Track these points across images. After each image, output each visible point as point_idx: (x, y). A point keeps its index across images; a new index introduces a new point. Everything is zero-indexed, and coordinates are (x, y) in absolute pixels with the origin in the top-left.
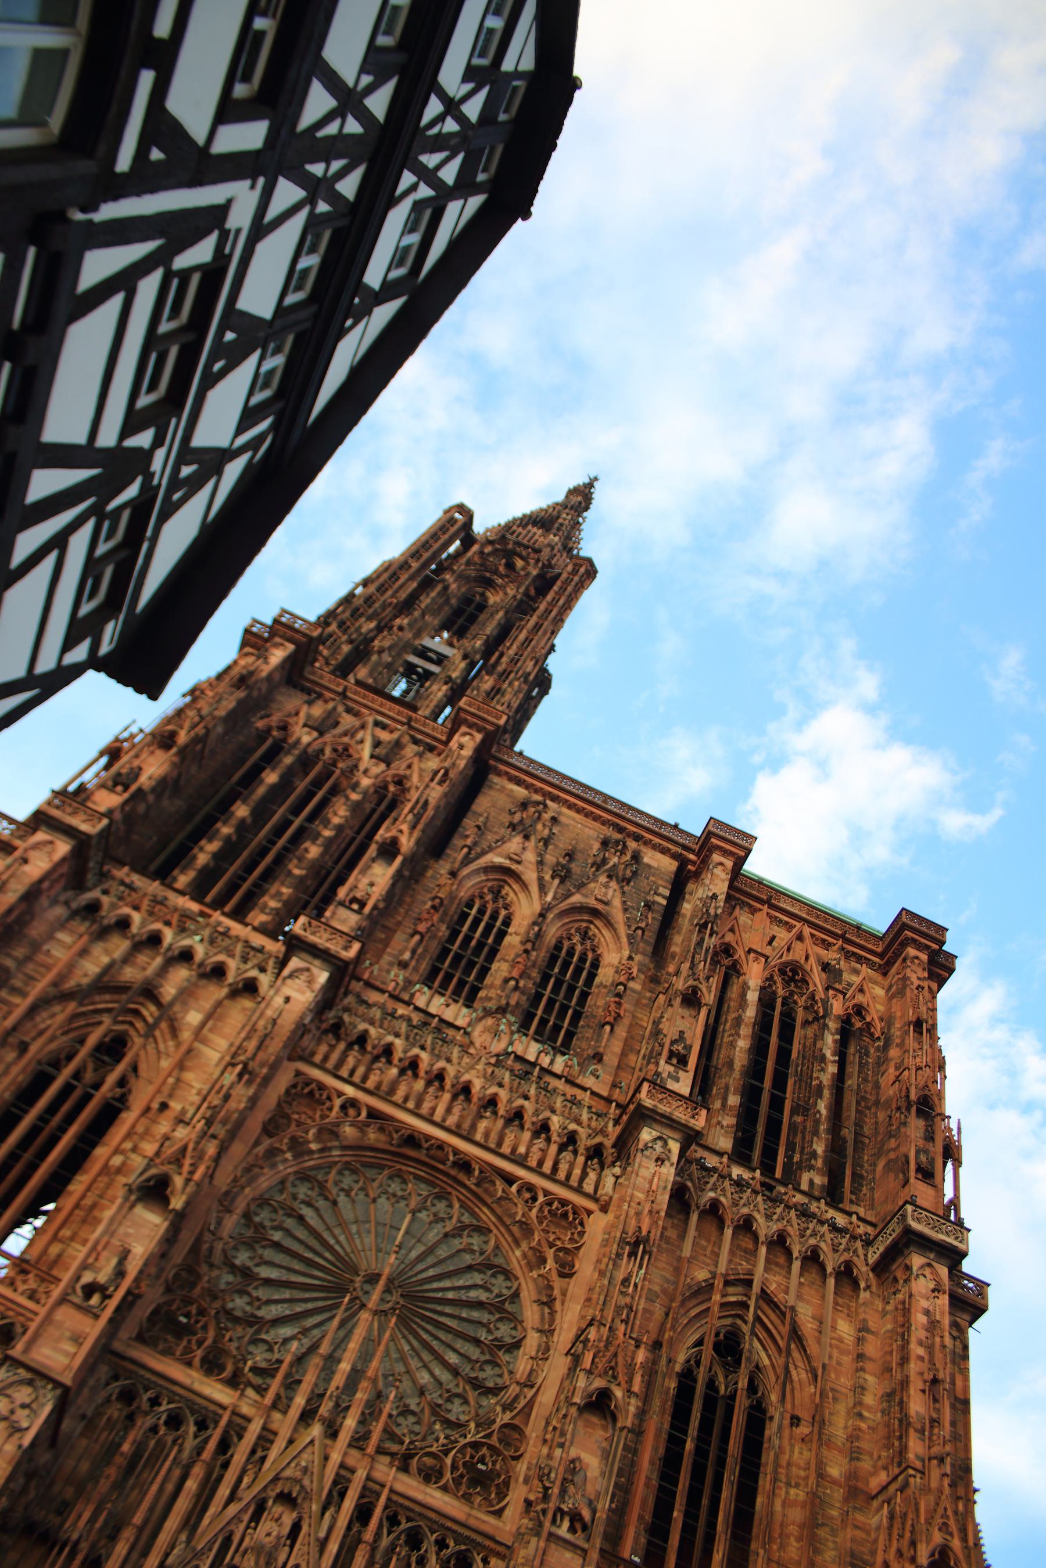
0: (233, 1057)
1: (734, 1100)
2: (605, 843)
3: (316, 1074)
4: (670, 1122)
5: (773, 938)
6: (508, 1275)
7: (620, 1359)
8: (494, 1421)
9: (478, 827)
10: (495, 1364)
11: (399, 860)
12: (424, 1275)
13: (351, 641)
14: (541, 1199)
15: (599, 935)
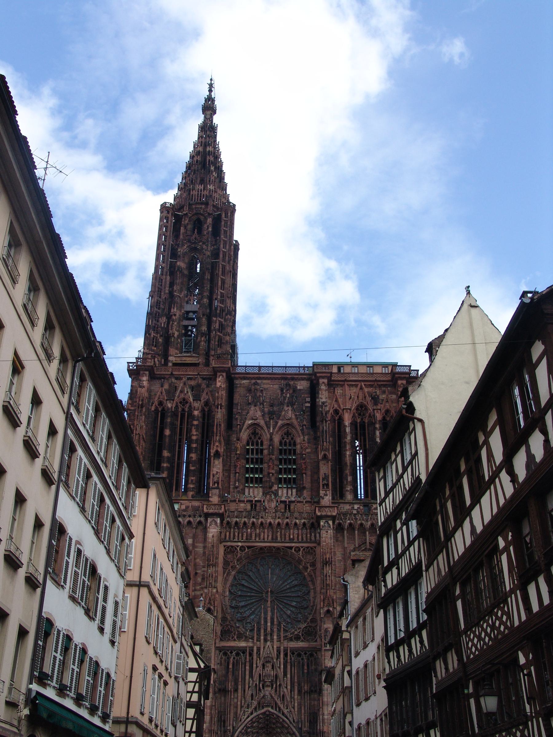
0: (208, 561)
1: (350, 478)
2: (282, 390)
3: (229, 544)
4: (326, 517)
5: (351, 397)
6: (300, 573)
7: (330, 600)
8: (308, 618)
9: (239, 412)
10: (305, 600)
11: (221, 458)
12: (279, 584)
13: (161, 336)
14: (302, 549)
15: (292, 432)
